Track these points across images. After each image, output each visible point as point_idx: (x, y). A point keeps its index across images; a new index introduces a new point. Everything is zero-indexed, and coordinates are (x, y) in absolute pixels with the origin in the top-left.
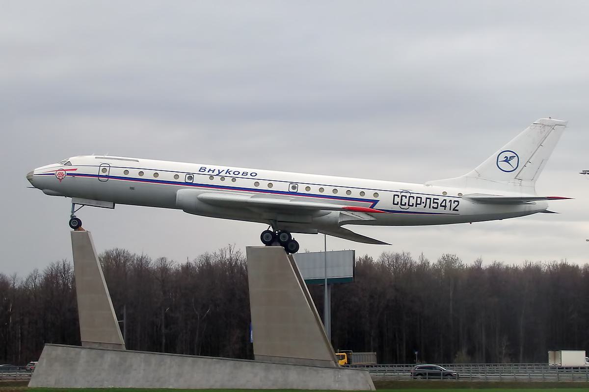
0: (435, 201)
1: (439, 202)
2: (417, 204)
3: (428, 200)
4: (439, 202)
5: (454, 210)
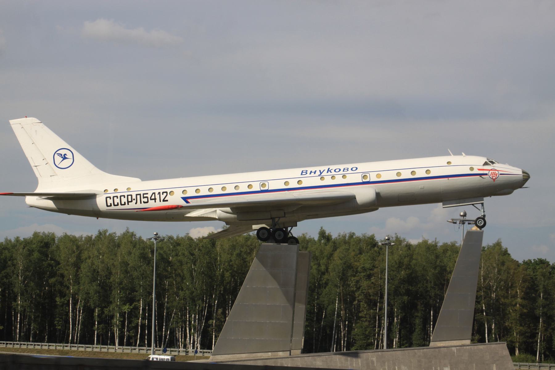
0: (145, 196)
1: (149, 196)
2: (128, 202)
3: (138, 196)
4: (149, 196)
5: (164, 201)
